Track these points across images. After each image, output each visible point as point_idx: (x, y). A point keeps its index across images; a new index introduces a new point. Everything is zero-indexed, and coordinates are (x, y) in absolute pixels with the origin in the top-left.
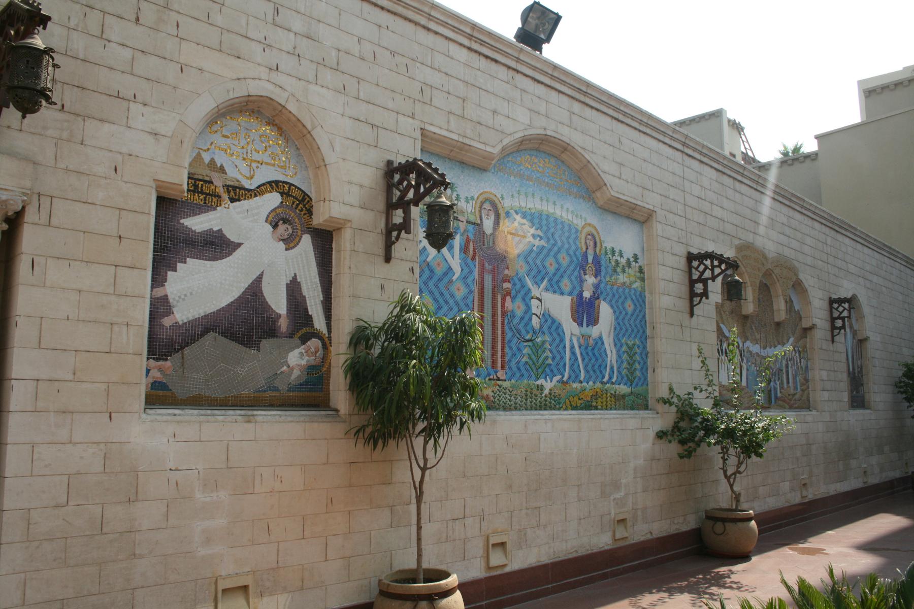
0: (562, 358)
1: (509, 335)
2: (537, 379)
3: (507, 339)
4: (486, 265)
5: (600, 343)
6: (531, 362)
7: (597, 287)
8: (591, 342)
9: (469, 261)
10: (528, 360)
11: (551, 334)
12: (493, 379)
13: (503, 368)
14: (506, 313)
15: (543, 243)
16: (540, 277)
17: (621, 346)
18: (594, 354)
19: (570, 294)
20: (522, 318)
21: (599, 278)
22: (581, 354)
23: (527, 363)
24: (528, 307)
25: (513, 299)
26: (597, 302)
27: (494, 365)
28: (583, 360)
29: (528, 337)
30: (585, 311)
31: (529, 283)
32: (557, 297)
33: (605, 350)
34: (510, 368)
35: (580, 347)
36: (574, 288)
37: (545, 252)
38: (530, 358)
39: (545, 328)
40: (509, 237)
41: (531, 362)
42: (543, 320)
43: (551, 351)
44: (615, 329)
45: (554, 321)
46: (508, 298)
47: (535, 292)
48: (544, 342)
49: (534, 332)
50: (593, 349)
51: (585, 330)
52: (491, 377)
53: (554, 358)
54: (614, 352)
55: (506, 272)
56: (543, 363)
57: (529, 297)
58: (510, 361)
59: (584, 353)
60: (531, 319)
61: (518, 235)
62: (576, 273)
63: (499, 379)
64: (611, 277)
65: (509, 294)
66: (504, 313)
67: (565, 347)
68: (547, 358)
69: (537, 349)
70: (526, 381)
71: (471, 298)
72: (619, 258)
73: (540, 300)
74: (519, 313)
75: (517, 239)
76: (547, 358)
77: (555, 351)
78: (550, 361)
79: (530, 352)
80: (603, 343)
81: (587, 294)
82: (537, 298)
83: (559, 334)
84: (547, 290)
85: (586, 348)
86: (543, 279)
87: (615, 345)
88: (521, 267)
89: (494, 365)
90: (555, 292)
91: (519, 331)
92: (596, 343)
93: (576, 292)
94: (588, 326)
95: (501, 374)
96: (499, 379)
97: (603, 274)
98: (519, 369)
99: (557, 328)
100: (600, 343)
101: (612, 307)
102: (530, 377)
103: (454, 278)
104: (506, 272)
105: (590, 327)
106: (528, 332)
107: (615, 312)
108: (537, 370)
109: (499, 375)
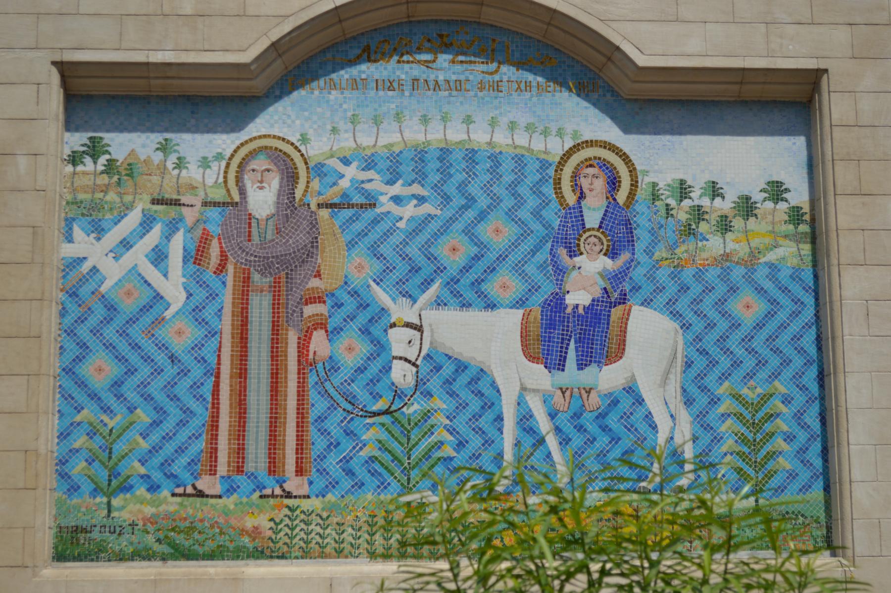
0: (488, 443)
1: (318, 405)
2: (407, 489)
3: (312, 415)
4: (256, 277)
5: (626, 403)
6: (386, 458)
7: (617, 278)
8: (594, 400)
9: (209, 276)
10: (377, 453)
11: (452, 394)
12: (273, 496)
13: (300, 471)
14: (313, 364)
15: (428, 208)
16: (418, 280)
17: (715, 401)
18: (605, 429)
19: (519, 303)
20: (360, 370)
21: (625, 257)
22: (558, 430)
23: (373, 459)
24: (380, 347)
25: (333, 334)
26: (616, 313)
27: (274, 467)
28: (565, 442)
29: (380, 405)
30: (574, 334)
31: (382, 296)
32: (476, 317)
33: (649, 416)
34: (323, 472)
35: (552, 416)
36: (534, 288)
37: (434, 226)
38: (382, 446)
39: (434, 384)
40: (324, 213)
41: (386, 458)
42: (425, 369)
43: (452, 431)
44: (688, 364)
45: (461, 367)
46: (318, 336)
47: (401, 310)
48: (427, 415)
49: (398, 394)
50: (602, 416)
51: (571, 374)
52: (268, 491)
53: (461, 445)
54: (685, 418)
55: (314, 283)
56: (427, 455)
57: (384, 322)
58: (322, 457)
59: (568, 429)
60: (387, 369)
61: (351, 206)
62: (543, 256)
63: (289, 495)
64: (672, 248)
65: (321, 325)
66: (305, 363)
67: (500, 418)
68: (440, 444)
69: (405, 430)
70: (369, 496)
71: (213, 344)
72: (706, 202)
73: (419, 328)
74: (349, 361)
75: (347, 213)
76: (440, 444)
77: (463, 429)
78: (448, 451)
79: (384, 436)
80: (640, 401)
81: (578, 297)
82: (408, 325)
83: (480, 394)
84: (439, 303)
85: (577, 415)
86: (427, 284)
87: (689, 402)
88: (360, 268)
89: (274, 467)
90: (465, 305)
91: (351, 399)
92: (615, 403)
93: (538, 299)
94: (581, 367)
95: (293, 484)
96: (289, 495)
97: (640, 246)
98: (350, 473)
99: (475, 380)
100: (626, 403)
101: (675, 315)
102: (384, 486)
103: (168, 314)
104: (314, 283)
105: (592, 369)
106: (377, 397)
107: (686, 327)
108: (406, 471)
109: (288, 486)
